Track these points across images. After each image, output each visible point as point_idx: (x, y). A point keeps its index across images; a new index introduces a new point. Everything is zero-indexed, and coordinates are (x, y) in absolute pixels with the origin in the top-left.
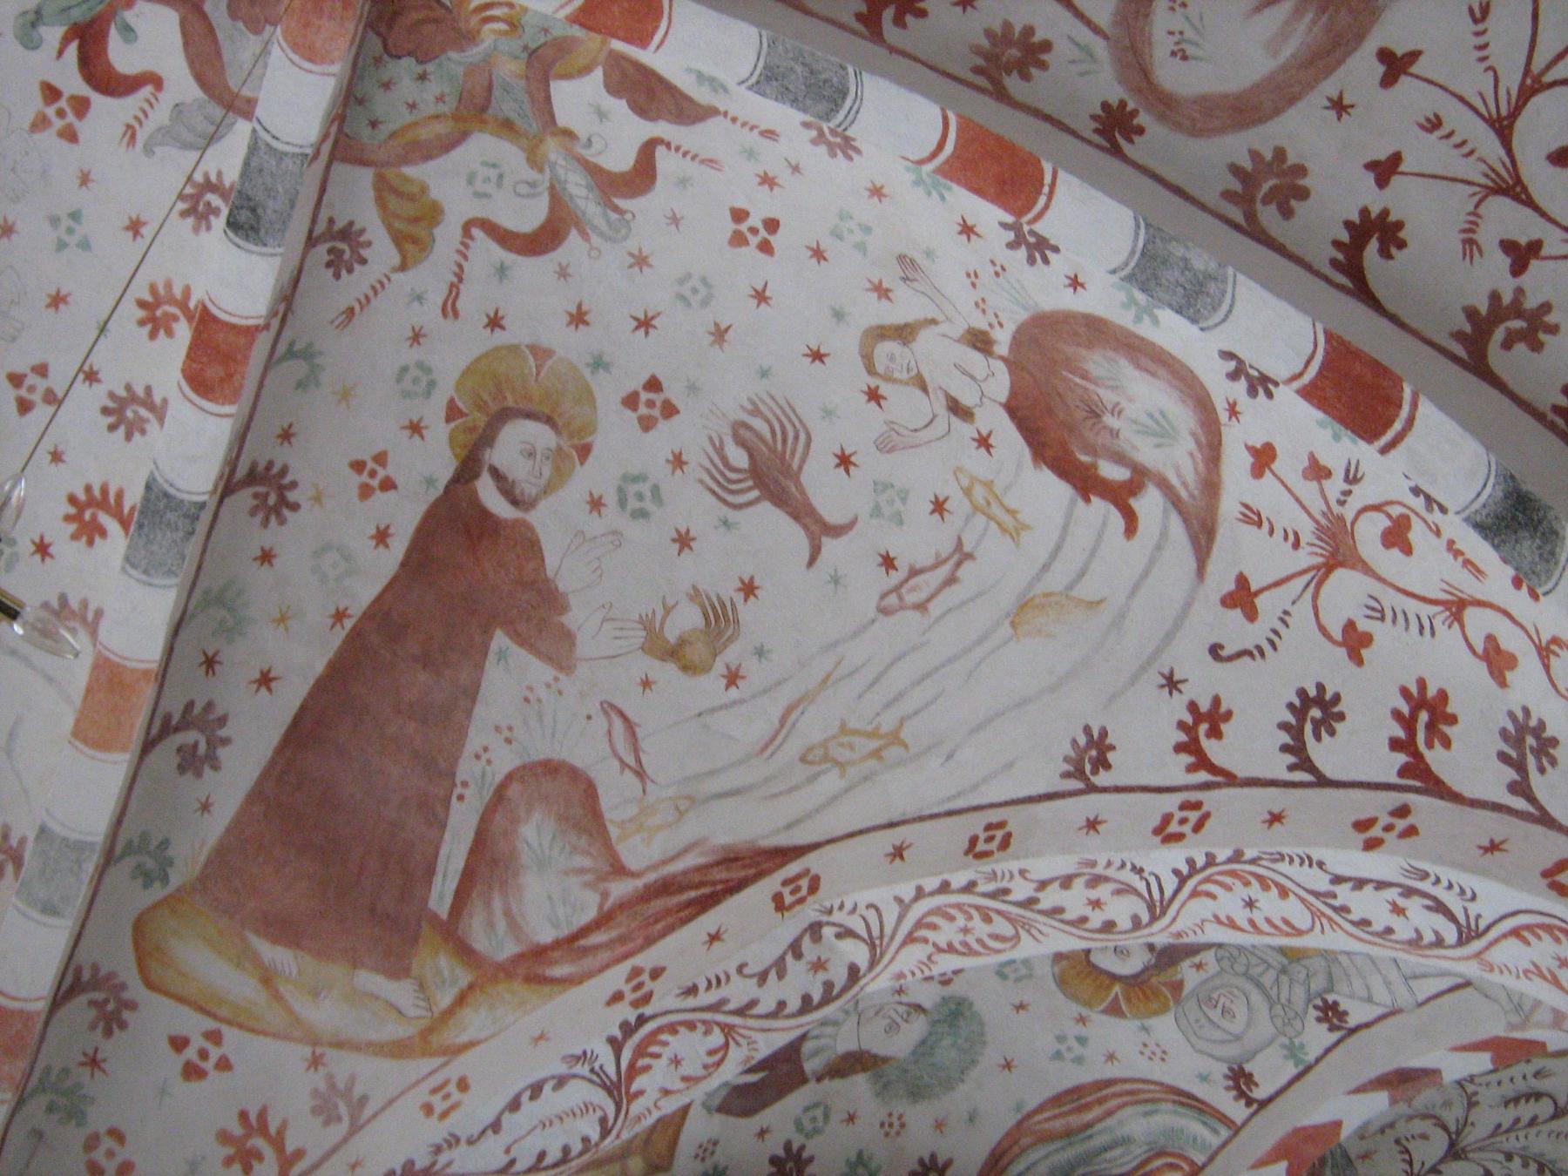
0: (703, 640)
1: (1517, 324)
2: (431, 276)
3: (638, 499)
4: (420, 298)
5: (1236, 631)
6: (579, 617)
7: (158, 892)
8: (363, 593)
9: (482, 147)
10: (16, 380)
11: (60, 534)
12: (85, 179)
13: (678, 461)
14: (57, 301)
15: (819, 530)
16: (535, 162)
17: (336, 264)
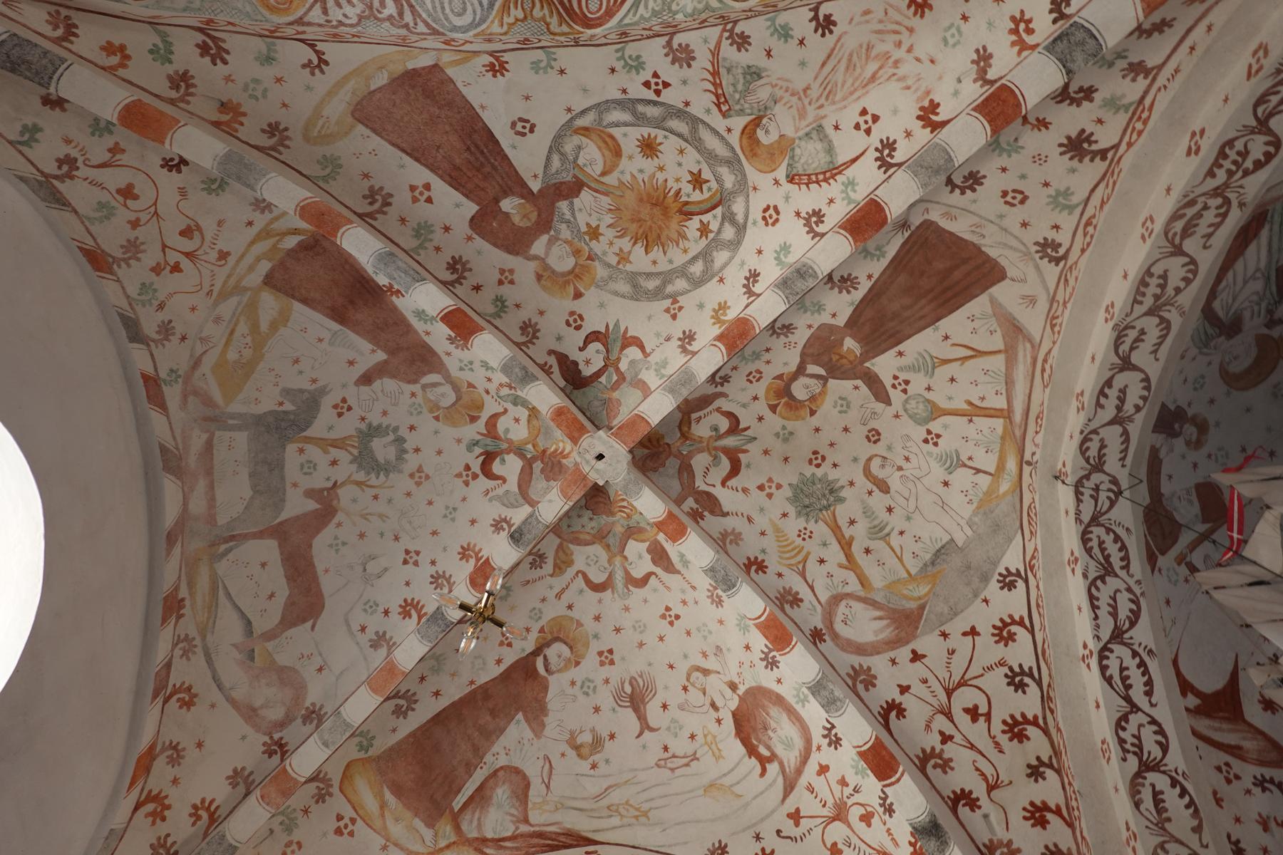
0: (589, 748)
1: (939, 761)
2: (558, 583)
3: (587, 687)
4: (551, 588)
5: (789, 828)
6: (551, 720)
7: (362, 755)
8: (483, 679)
9: (597, 550)
10: (407, 552)
11: (395, 610)
12: (464, 499)
13: (607, 681)
14: (434, 533)
15: (645, 726)
16: (610, 561)
17: (533, 565)
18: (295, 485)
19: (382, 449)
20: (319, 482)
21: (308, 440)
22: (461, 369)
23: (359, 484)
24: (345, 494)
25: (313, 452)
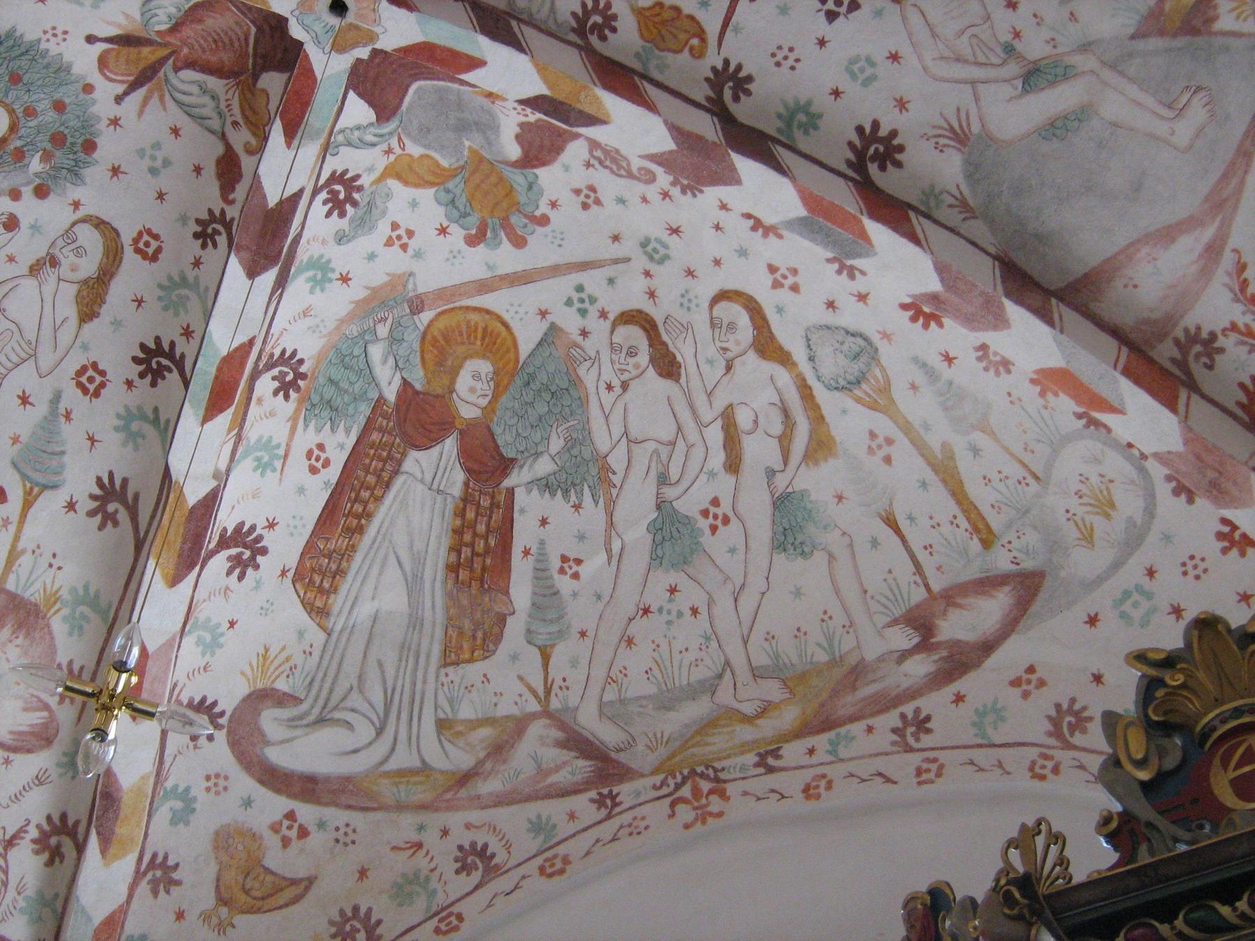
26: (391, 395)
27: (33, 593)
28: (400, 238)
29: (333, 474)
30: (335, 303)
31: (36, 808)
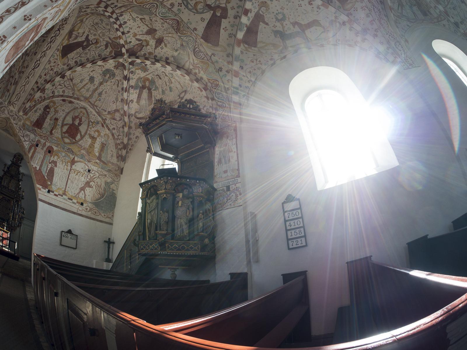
10: (299, 6)
18: (293, 30)
19: (280, 17)
20: (291, 27)
21: (284, 30)
22: (256, 8)
23: (289, 19)
24: (292, 21)
25: (285, 29)
26: (141, 86)
27: (118, 109)
28: (138, 74)
29: (138, 93)
30: (134, 81)
31: (121, 125)
